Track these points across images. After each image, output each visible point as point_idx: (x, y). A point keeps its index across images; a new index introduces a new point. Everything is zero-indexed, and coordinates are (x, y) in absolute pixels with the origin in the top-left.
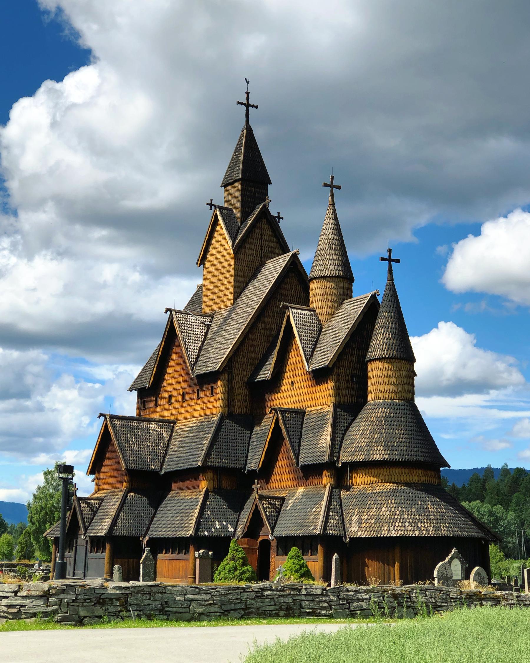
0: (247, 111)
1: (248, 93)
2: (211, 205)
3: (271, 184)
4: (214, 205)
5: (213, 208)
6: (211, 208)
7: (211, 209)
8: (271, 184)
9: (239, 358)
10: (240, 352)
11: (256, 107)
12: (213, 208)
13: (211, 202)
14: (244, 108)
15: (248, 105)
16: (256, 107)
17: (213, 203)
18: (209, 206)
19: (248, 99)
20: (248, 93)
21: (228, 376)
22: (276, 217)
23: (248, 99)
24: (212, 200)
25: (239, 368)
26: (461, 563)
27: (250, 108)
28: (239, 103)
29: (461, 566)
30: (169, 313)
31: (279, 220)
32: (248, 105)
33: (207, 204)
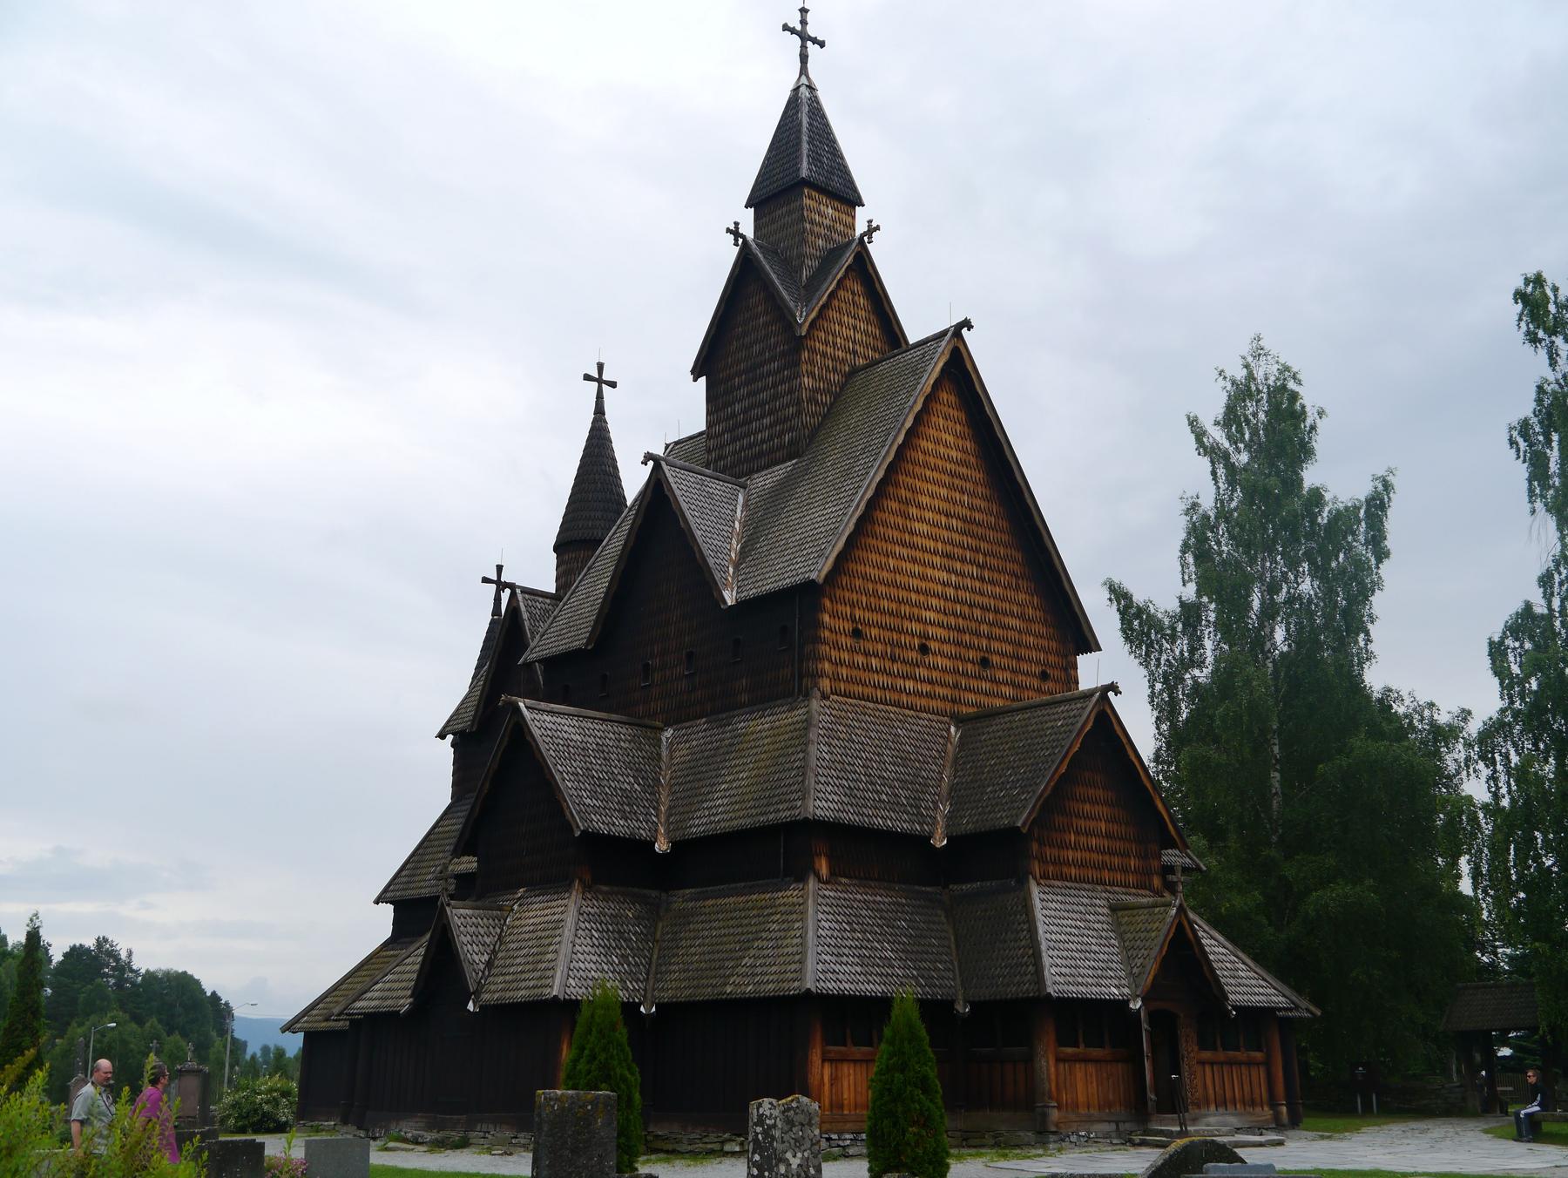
0: (804, 47)
1: (804, 11)
2: (735, 232)
3: (863, 205)
5: (740, 241)
6: (736, 240)
7: (736, 244)
8: (863, 205)
11: (822, 45)
14: (797, 40)
15: (804, 37)
16: (822, 45)
18: (732, 236)
19: (804, 22)
20: (804, 11)
23: (804, 22)
24: (736, 224)
27: (809, 44)
28: (786, 28)
32: (804, 37)
33: (728, 230)
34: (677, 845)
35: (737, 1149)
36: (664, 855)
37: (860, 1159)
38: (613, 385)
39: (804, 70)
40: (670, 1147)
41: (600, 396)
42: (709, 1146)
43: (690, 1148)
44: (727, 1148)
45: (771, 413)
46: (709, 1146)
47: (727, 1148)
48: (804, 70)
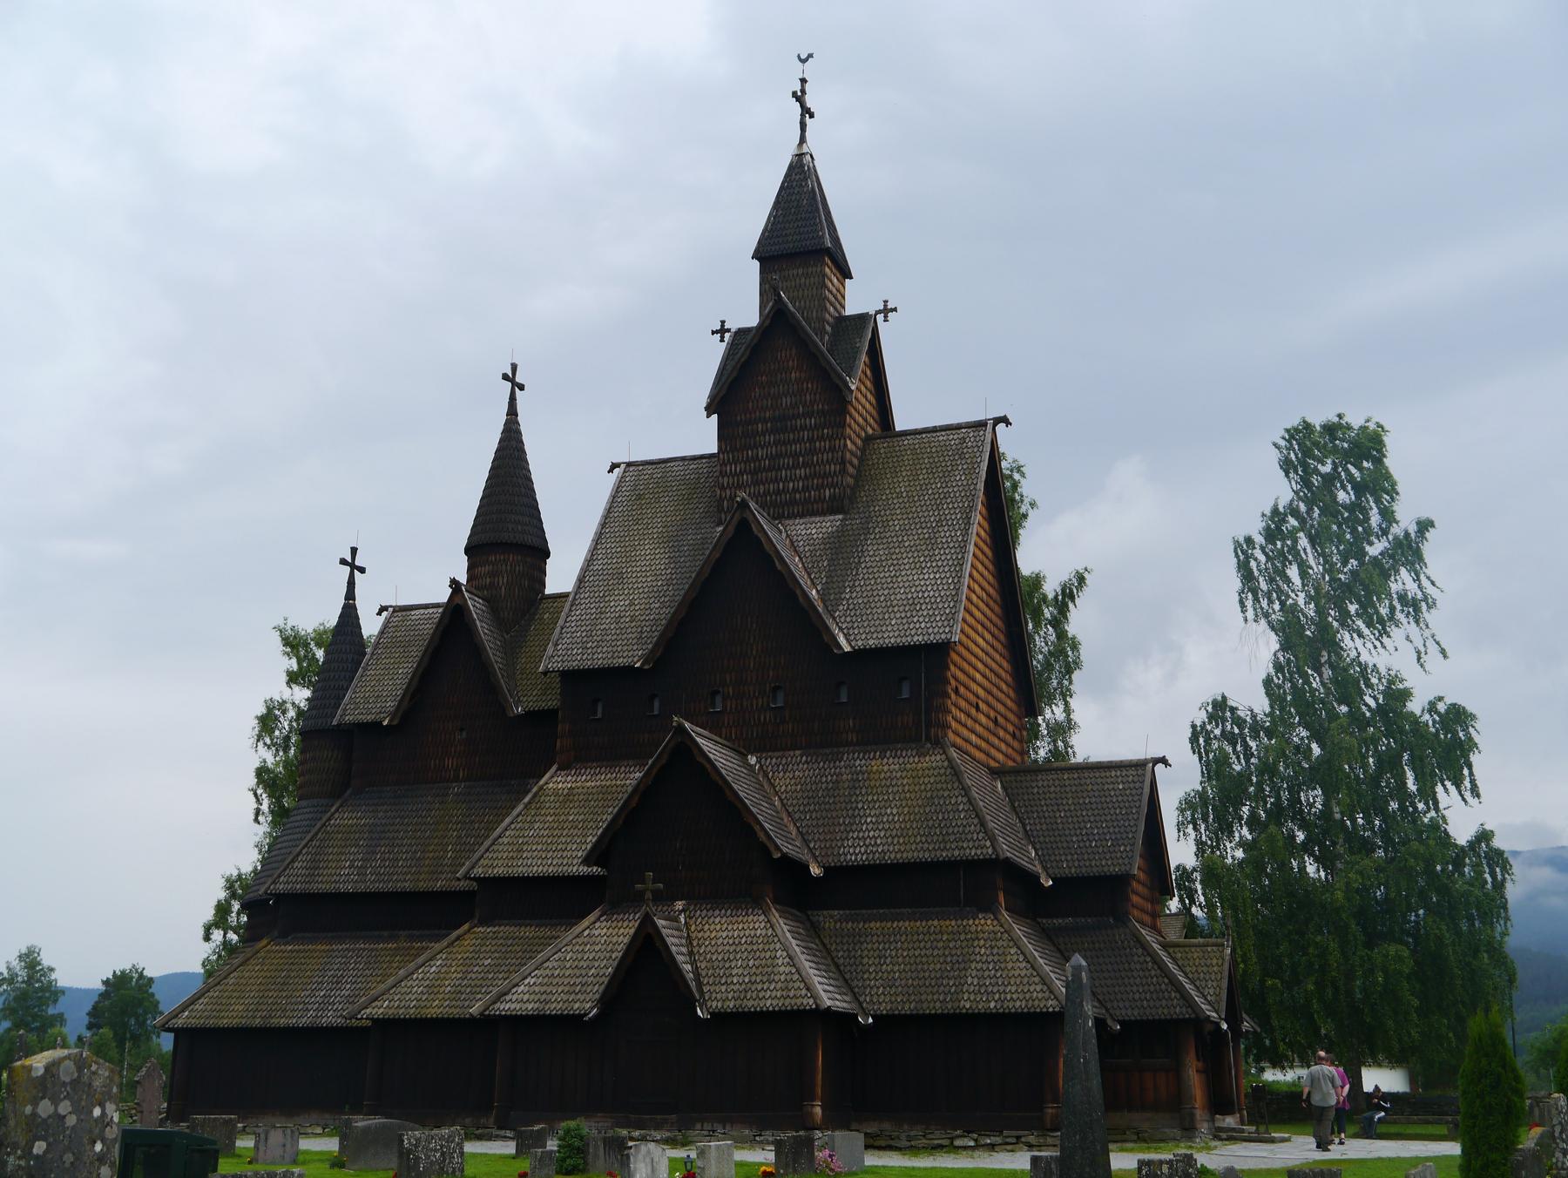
1: (803, 81)
4: (729, 330)
7: (722, 340)
12: (727, 335)
20: (803, 81)
22: (878, 312)
31: (886, 317)
34: (828, 870)
35: (972, 1143)
36: (818, 879)
37: (888, 1153)
38: (362, 570)
39: (803, 140)
40: (883, 1143)
41: (351, 584)
42: (936, 1142)
43: (908, 1144)
44: (958, 1143)
45: (805, 465)
46: (936, 1142)
47: (958, 1143)
48: (803, 140)
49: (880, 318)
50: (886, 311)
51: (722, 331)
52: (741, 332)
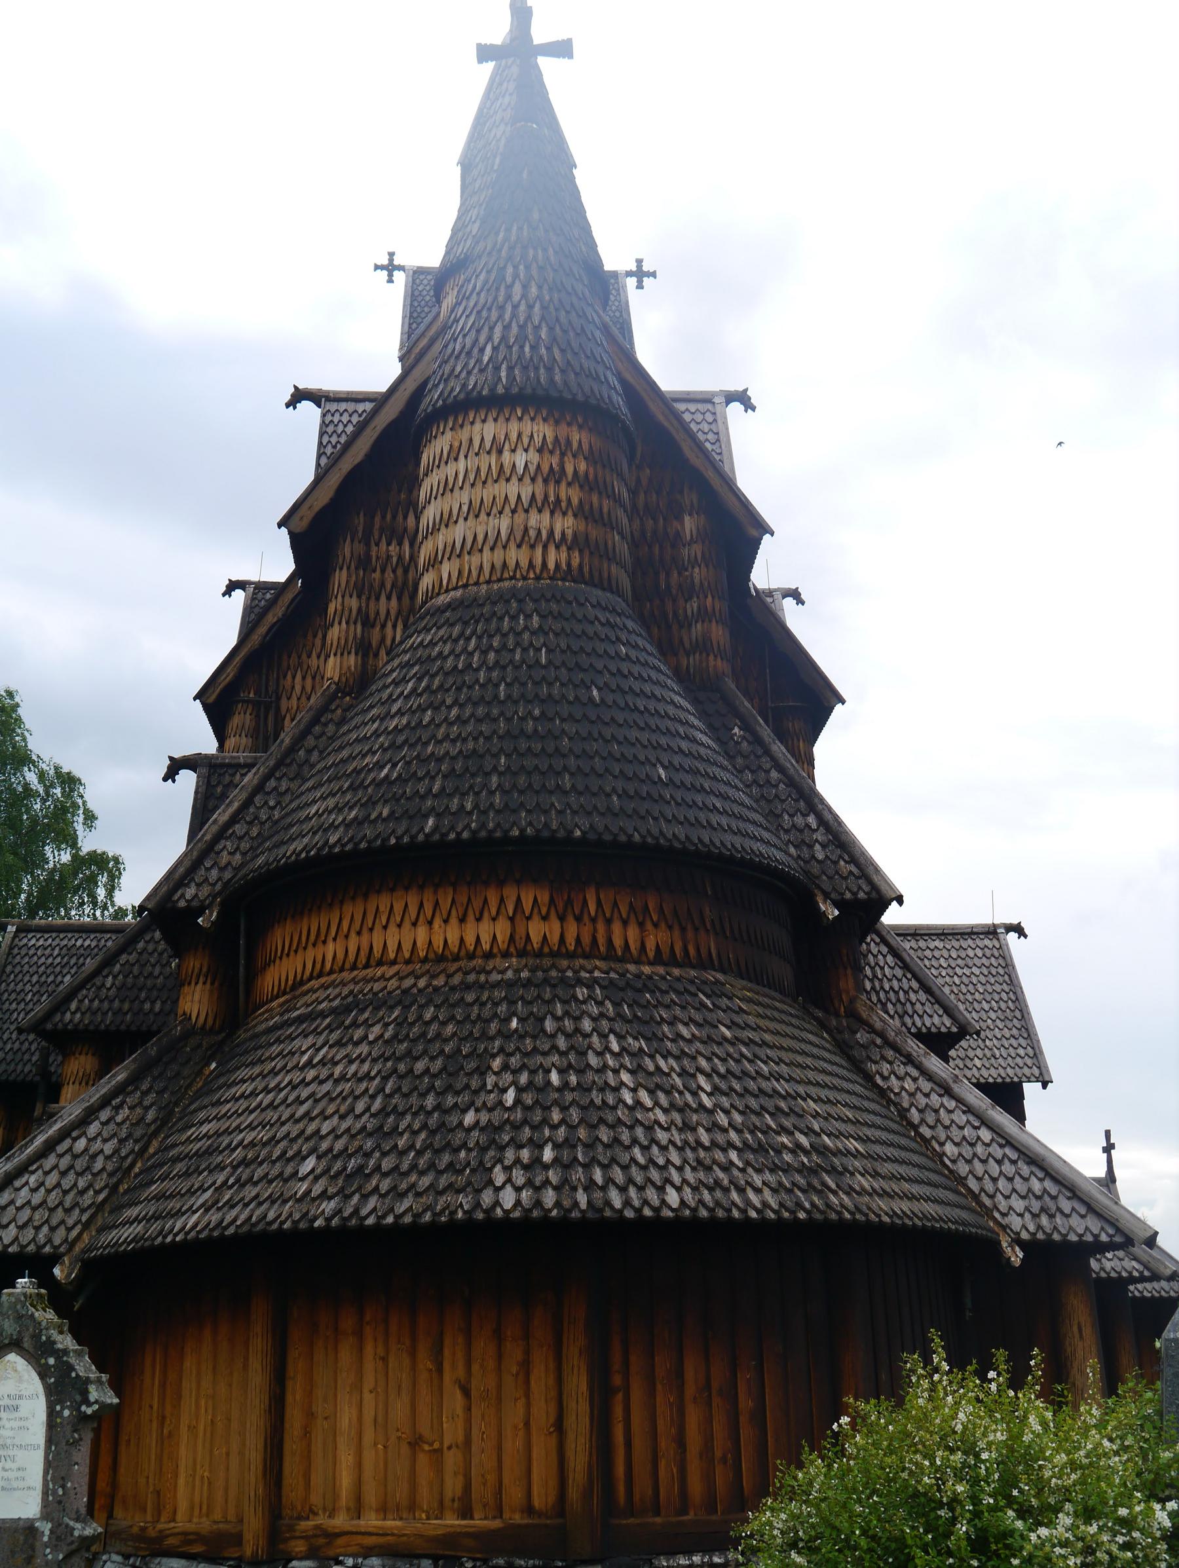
2: (390, 268)
4: (401, 268)
5: (399, 276)
6: (390, 275)
7: (390, 281)
9: (309, 656)
10: (310, 637)
12: (399, 276)
13: (391, 260)
17: (396, 263)
18: (385, 273)
21: (257, 716)
22: (629, 274)
24: (391, 255)
25: (308, 689)
26: (49, 1391)
29: (52, 1414)
30: (239, 595)
33: (377, 267)
49: (631, 282)
50: (640, 274)
51: (390, 268)
52: (417, 275)
